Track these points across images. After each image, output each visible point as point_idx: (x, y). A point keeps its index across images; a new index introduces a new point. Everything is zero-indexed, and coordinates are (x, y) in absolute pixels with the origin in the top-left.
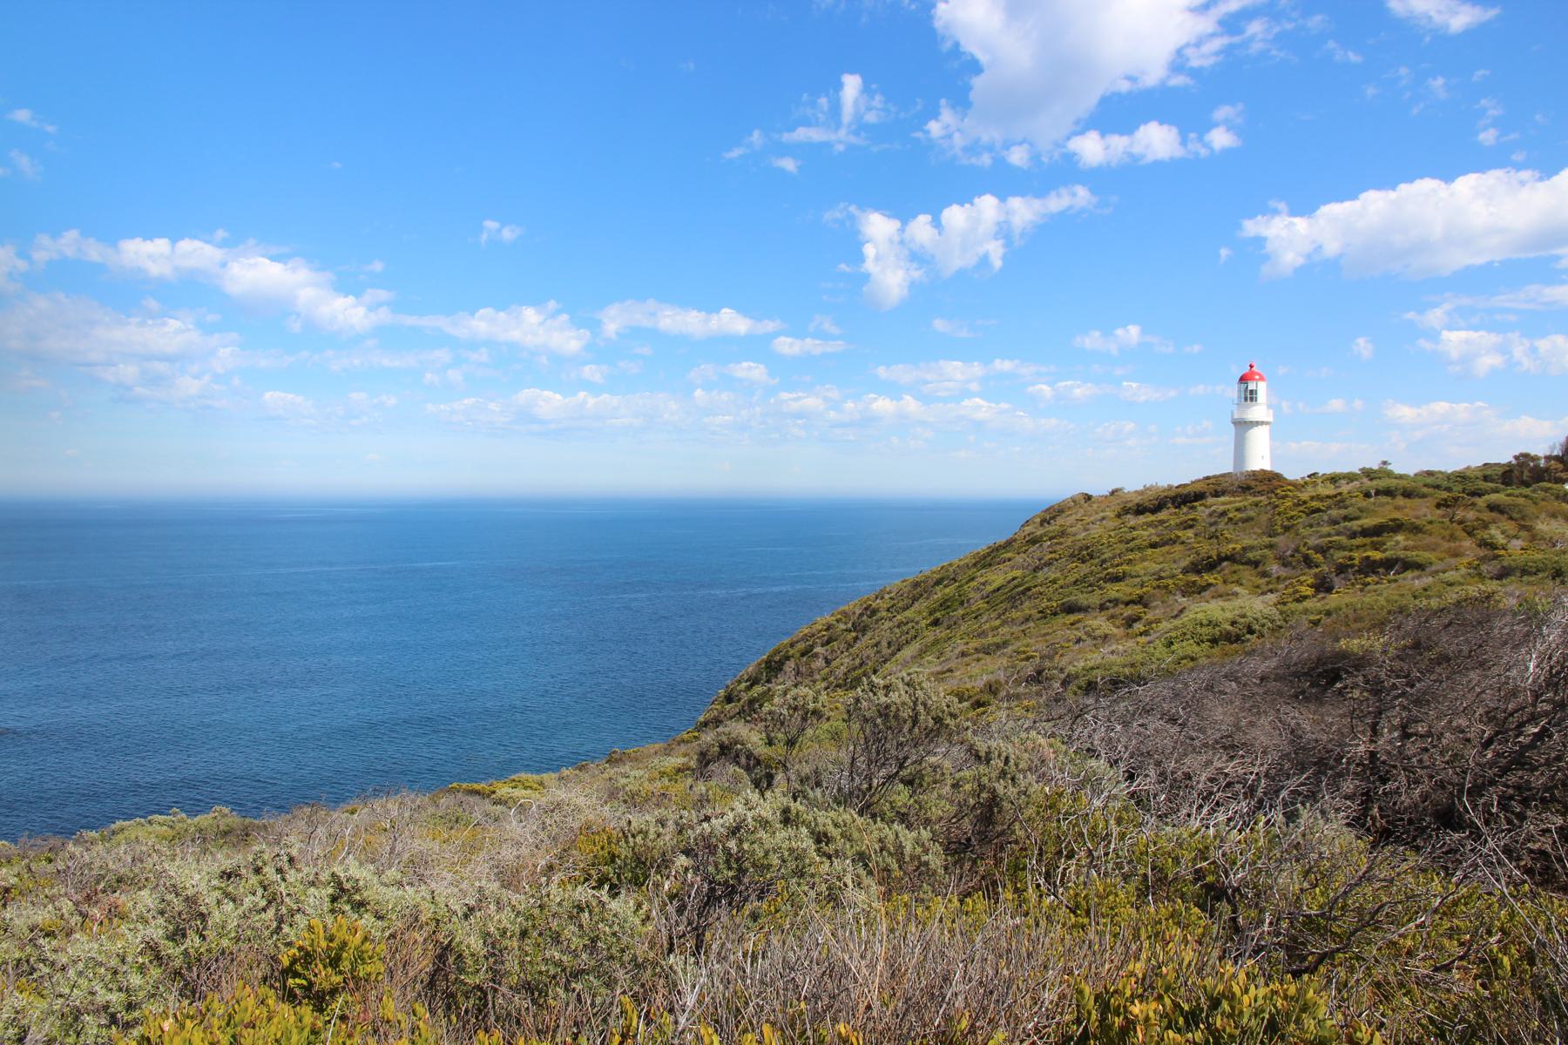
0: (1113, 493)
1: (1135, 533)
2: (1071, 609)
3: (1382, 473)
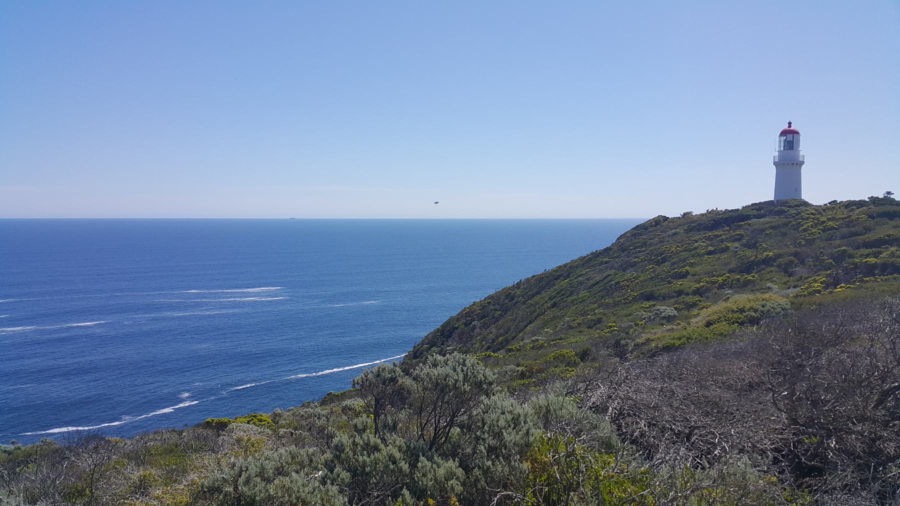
0: (685, 214)
1: (696, 245)
2: (649, 297)
3: (887, 200)
